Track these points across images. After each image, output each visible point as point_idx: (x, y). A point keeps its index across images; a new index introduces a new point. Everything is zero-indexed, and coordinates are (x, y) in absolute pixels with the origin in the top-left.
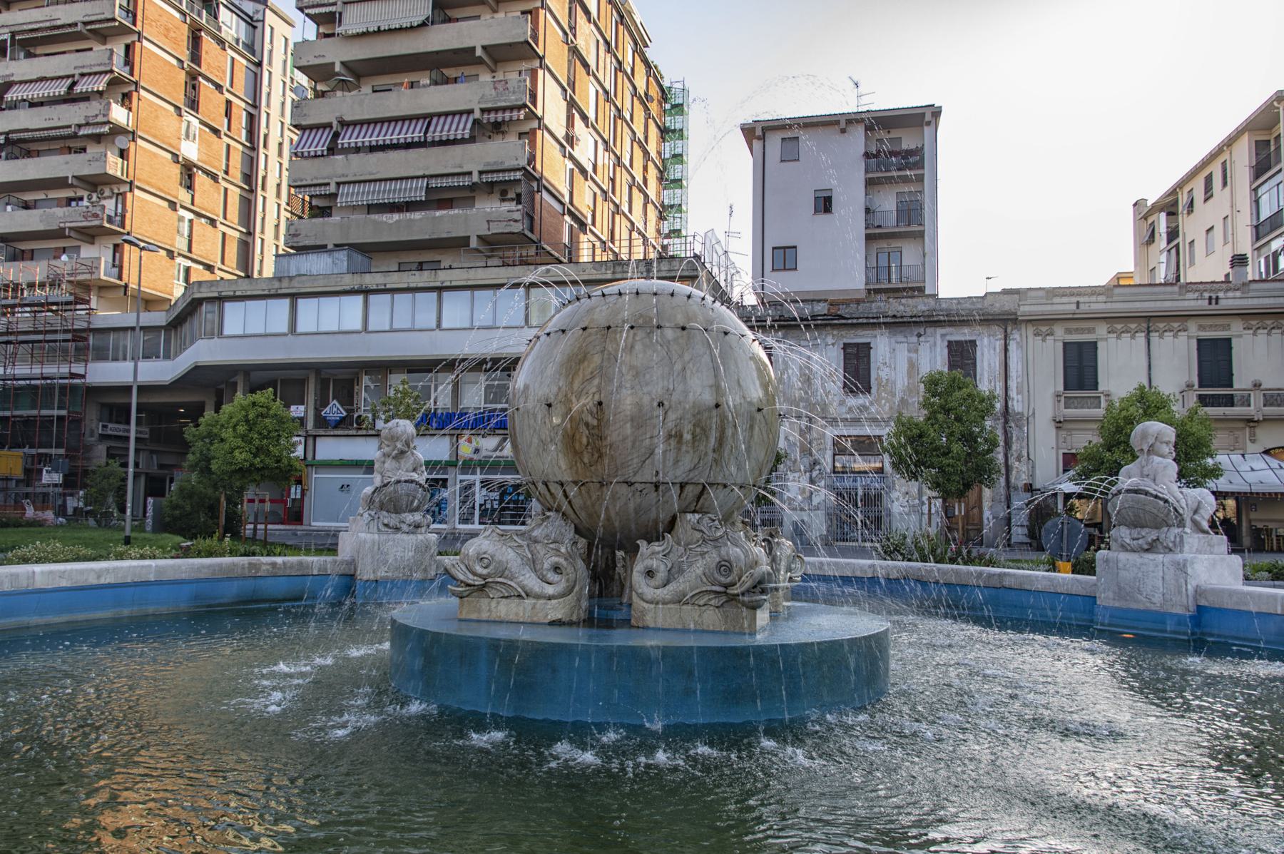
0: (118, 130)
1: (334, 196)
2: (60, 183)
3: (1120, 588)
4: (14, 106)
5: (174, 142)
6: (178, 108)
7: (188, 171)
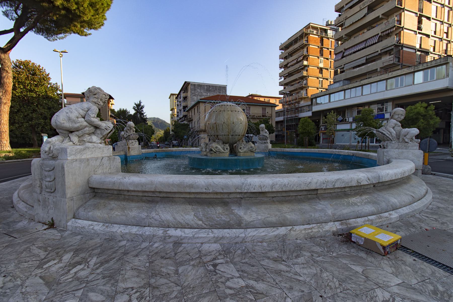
0: (306, 66)
1: (343, 68)
2: (296, 80)
4: (289, 67)
5: (317, 64)
6: (318, 57)
7: (321, 70)
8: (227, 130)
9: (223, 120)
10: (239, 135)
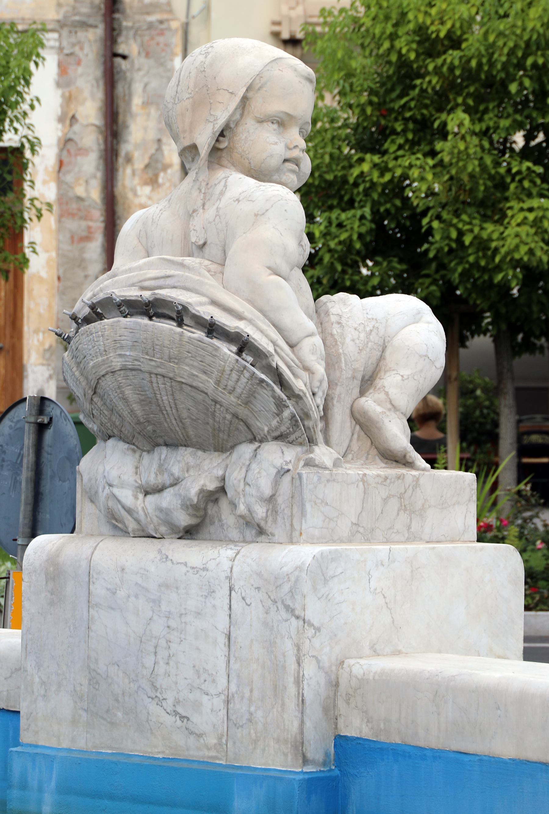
3: (94, 679)
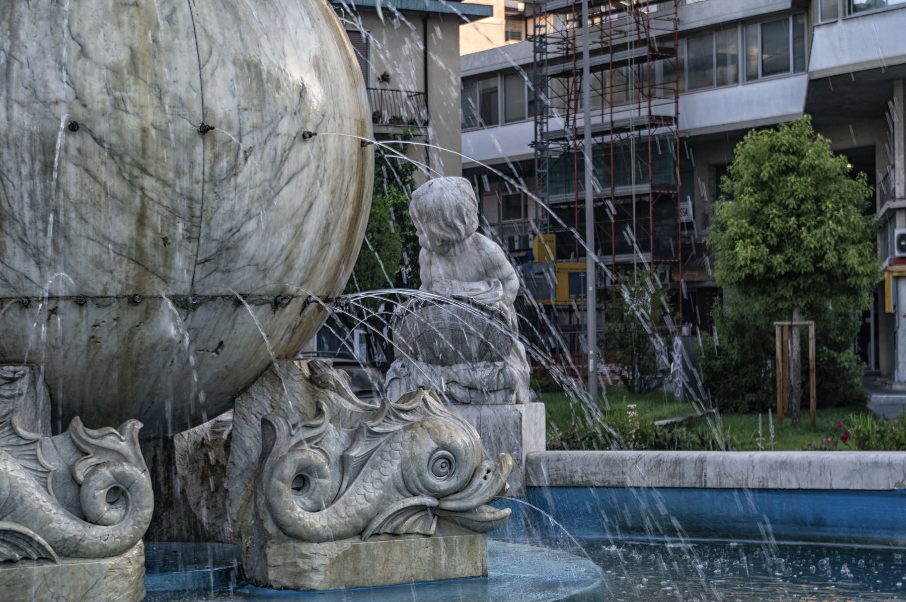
8: (122, 228)
9: (59, 89)
10: (278, 302)
